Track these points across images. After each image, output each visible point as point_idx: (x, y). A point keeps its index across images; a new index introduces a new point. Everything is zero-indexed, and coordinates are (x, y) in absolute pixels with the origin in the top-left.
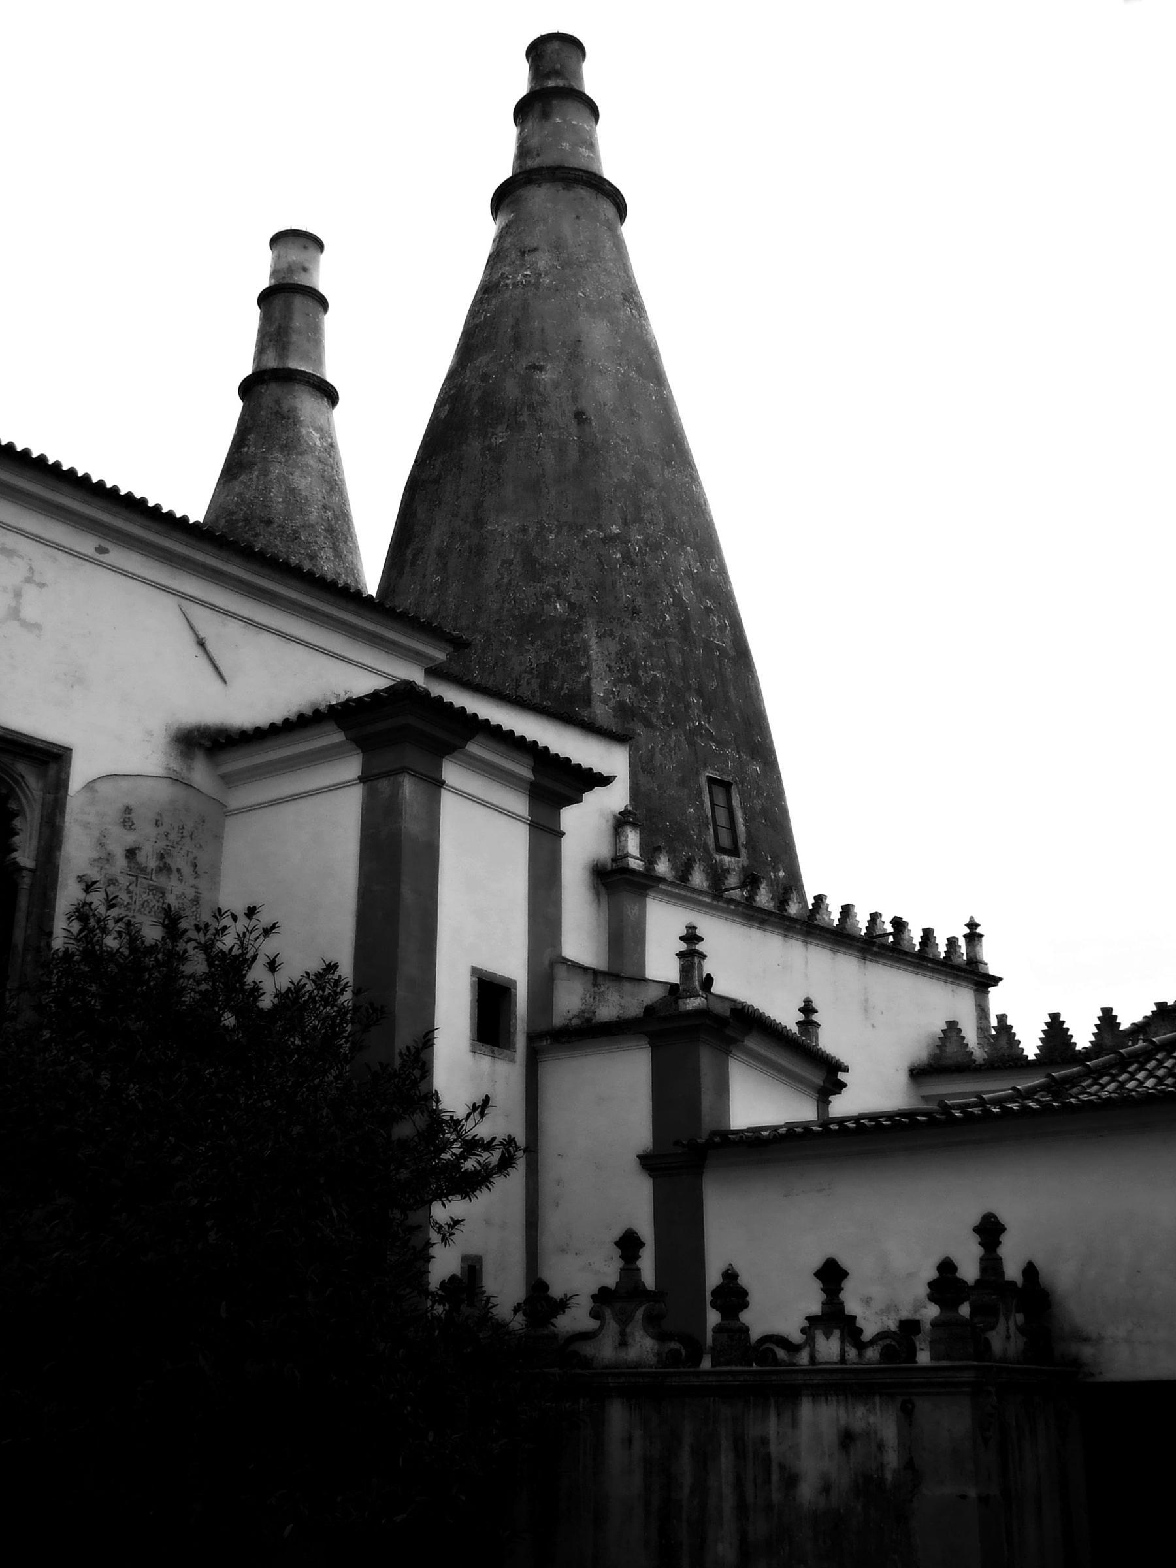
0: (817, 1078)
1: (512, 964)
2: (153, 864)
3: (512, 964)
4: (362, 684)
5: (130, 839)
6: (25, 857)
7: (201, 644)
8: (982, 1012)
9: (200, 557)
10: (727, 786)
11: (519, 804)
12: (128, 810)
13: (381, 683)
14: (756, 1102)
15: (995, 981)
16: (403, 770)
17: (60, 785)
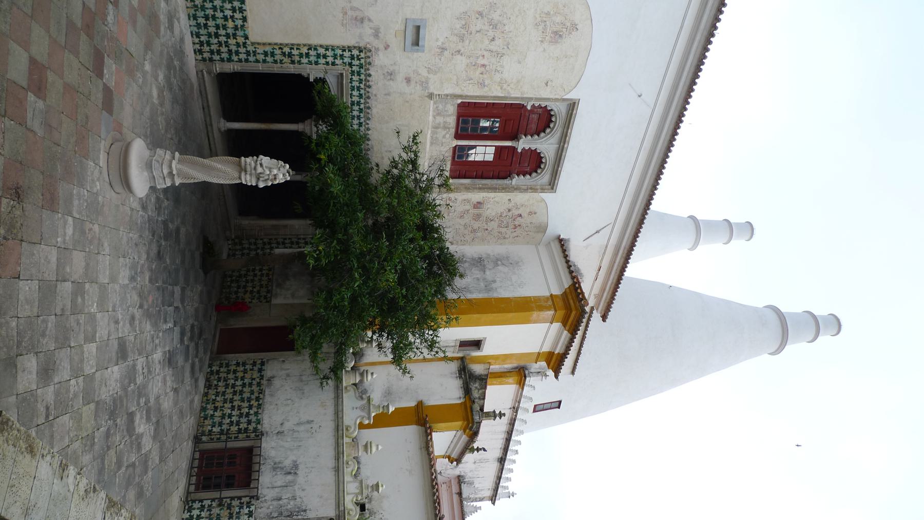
0: (454, 455)
1: (487, 350)
2: (517, 223)
4: (586, 287)
6: (517, 180)
7: (597, 232)
8: (481, 500)
9: (630, 228)
10: (559, 407)
11: (546, 348)
12: (535, 213)
13: (586, 295)
15: (494, 504)
16: (556, 311)
17: (543, 190)
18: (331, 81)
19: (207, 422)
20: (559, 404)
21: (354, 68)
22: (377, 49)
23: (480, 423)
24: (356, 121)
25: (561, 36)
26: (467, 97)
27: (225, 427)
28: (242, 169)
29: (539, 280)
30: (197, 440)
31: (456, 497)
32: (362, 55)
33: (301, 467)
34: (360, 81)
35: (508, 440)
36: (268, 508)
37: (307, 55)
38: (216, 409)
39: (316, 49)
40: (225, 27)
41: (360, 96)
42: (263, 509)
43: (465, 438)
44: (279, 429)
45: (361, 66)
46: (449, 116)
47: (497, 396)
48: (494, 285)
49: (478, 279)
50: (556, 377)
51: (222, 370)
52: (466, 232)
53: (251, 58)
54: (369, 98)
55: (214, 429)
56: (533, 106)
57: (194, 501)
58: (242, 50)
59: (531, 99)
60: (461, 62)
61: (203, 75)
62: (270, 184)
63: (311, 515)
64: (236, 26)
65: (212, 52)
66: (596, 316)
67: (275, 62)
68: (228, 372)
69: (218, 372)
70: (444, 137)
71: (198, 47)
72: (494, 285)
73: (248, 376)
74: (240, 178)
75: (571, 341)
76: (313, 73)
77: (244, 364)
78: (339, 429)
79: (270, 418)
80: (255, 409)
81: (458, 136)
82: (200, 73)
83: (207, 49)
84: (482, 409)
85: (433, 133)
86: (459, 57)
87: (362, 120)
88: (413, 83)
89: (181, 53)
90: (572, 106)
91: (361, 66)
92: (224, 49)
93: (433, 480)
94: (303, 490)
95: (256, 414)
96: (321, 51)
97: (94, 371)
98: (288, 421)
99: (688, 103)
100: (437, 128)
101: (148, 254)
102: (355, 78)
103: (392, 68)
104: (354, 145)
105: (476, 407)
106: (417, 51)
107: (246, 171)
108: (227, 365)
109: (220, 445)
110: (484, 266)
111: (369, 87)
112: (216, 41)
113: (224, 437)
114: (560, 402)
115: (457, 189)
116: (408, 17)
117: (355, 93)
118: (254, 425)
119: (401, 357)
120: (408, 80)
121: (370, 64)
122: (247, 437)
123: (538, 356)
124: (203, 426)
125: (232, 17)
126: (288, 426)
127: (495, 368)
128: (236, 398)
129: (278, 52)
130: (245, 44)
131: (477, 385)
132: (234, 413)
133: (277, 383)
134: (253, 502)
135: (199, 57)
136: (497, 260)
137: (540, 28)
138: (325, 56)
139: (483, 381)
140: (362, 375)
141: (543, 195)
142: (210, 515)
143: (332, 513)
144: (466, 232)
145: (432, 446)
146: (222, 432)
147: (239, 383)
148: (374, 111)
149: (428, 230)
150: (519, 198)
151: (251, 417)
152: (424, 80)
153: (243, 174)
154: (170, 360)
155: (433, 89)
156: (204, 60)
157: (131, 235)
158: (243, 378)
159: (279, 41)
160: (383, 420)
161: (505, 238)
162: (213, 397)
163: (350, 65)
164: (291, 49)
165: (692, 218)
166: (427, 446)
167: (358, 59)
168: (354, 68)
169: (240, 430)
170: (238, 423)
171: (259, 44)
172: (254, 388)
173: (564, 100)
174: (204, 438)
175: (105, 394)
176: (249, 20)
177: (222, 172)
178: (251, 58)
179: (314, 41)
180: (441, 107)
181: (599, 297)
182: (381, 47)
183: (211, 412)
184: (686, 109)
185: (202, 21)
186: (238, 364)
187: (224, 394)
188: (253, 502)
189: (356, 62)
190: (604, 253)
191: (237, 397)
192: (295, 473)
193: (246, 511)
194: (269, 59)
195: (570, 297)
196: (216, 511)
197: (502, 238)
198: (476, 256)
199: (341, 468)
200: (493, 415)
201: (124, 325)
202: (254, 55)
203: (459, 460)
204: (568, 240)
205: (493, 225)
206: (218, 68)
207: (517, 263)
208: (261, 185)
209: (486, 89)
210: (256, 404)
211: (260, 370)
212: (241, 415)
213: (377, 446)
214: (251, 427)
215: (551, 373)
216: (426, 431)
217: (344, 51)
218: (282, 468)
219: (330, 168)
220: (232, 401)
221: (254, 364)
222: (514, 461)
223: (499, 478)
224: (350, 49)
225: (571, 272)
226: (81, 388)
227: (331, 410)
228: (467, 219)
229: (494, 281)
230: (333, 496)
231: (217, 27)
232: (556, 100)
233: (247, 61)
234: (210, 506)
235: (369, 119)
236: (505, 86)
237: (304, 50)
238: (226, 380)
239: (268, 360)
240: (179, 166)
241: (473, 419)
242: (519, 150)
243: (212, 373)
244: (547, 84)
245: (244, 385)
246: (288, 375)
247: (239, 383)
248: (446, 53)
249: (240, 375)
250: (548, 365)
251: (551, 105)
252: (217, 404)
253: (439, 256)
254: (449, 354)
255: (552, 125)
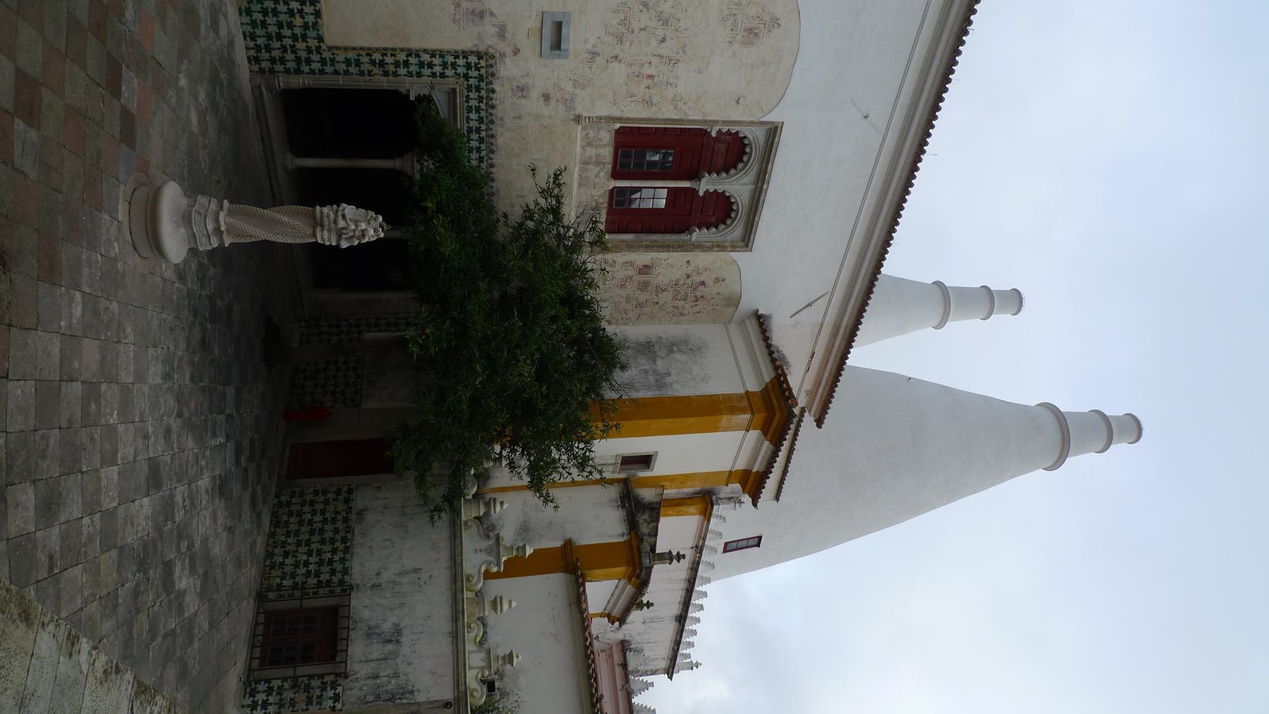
1: (659, 469)
2: (698, 294)
3: (660, 469)
4: (794, 380)
5: (709, 282)
6: (697, 235)
7: (809, 305)
8: (654, 673)
10: (758, 545)
11: (741, 465)
13: (795, 392)
14: (599, 593)
15: (671, 678)
16: (753, 414)
17: (734, 248)
18: (440, 98)
19: (274, 573)
20: (758, 541)
21: (472, 81)
22: (503, 55)
23: (650, 568)
24: (474, 155)
25: (756, 35)
26: (627, 120)
27: (299, 579)
28: (317, 223)
29: (728, 371)
30: (261, 597)
31: (618, 670)
32: (483, 63)
33: (405, 632)
34: (480, 99)
35: (689, 591)
36: (361, 689)
37: (406, 64)
38: (286, 554)
39: (417, 55)
40: (290, 26)
41: (480, 120)
42: (354, 691)
43: (630, 589)
44: (375, 581)
45: (480, 78)
46: (604, 146)
47: (674, 532)
48: (668, 380)
49: (646, 372)
50: (755, 504)
51: (294, 500)
52: (629, 307)
53: (328, 69)
54: (492, 122)
55: (285, 583)
56: (719, 132)
57: (258, 682)
58: (315, 57)
59: (716, 122)
60: (619, 72)
61: (261, 92)
62: (356, 243)
63: (420, 698)
64: (306, 24)
65: (273, 60)
66: (809, 420)
67: (362, 73)
68: (303, 504)
69: (289, 504)
70: (597, 176)
71: (253, 53)
72: (668, 380)
73: (330, 508)
74: (314, 235)
75: (775, 455)
76: (415, 88)
77: (325, 492)
78: (457, 580)
79: (363, 565)
80: (340, 555)
81: (616, 175)
82: (256, 89)
83: (267, 56)
84: (653, 548)
85: (582, 170)
86: (616, 64)
87: (483, 153)
88: (553, 102)
89: (228, 62)
90: (774, 131)
91: (480, 78)
92: (290, 56)
93: (587, 648)
94: (409, 664)
95: (343, 560)
96: (426, 58)
97: (114, 504)
98: (387, 569)
99: (933, 127)
100: (587, 163)
101: (188, 341)
102: (473, 95)
103: (523, 81)
104: (473, 188)
105: (646, 547)
106: (559, 57)
107: (322, 226)
108: (302, 494)
109: (294, 604)
110: (654, 353)
111: (493, 107)
112: (278, 45)
113: (298, 593)
114: (760, 538)
115: (617, 248)
116: (545, 9)
117: (473, 116)
118: (339, 576)
119: (541, 480)
120: (546, 97)
121: (493, 75)
122: (331, 592)
123: (730, 477)
124: (268, 579)
125: (300, 11)
126: (387, 576)
127: (670, 492)
128: (314, 539)
129: (365, 59)
130: (318, 48)
131: (646, 516)
132: (312, 560)
133: (370, 517)
134: (340, 681)
135: (256, 68)
136: (672, 344)
137: (729, 23)
138: (431, 65)
139: (654, 511)
140: (487, 505)
141: (734, 255)
142: (281, 700)
143: (448, 695)
144: (629, 307)
145: (586, 601)
146: (295, 587)
147: (318, 518)
148: (500, 141)
149: (577, 305)
150: (702, 259)
151: (335, 565)
152: (567, 97)
153: (318, 230)
154: (221, 488)
155: (582, 108)
156: (262, 71)
157: (164, 316)
158: (323, 512)
159: (367, 45)
160: (518, 567)
161: (682, 315)
162: (283, 538)
163: (466, 77)
164: (384, 55)
165: (938, 284)
166: (578, 600)
167: (477, 69)
168: (472, 81)
169: (320, 582)
170: (317, 574)
171: (338, 48)
172: (339, 525)
173: (762, 123)
174: (271, 595)
175: (131, 537)
176: (325, 16)
177: (288, 227)
178: (328, 69)
179: (416, 44)
180: (592, 134)
181: (812, 395)
182: (509, 51)
183: (281, 559)
184: (929, 135)
185: (258, 17)
186: (316, 493)
187: (297, 533)
188: (340, 681)
189: (473, 73)
190: (819, 334)
191: (315, 538)
192: (398, 641)
193: (331, 694)
194: (353, 69)
195: (772, 394)
196: (288, 695)
197: (678, 314)
198: (642, 339)
199: (460, 632)
200: (669, 557)
201: (157, 440)
202: (333, 64)
203: (622, 620)
204: (767, 317)
205: (666, 297)
206: (282, 82)
207: (699, 349)
208: (344, 245)
209: (654, 109)
210: (341, 547)
211: (347, 501)
212: (321, 563)
213: (510, 602)
214: (335, 579)
215: (747, 499)
216: (577, 581)
217: (457, 57)
218: (379, 635)
219: (438, 221)
220: (308, 543)
221: (339, 492)
222: (698, 620)
223: (677, 643)
224: (465, 54)
225: (773, 361)
226: (98, 528)
227: (444, 555)
228: (631, 289)
229: (669, 374)
230: (450, 671)
231: (280, 25)
232: (752, 123)
233: (322, 72)
234: (279, 688)
235: (492, 152)
236: (680, 105)
237: (402, 57)
238: (299, 514)
239: (357, 487)
240: (230, 220)
241: (641, 563)
242: (701, 193)
243: (280, 505)
244: (738, 102)
245: (325, 521)
246: (386, 507)
247: (318, 518)
248: (598, 59)
249: (319, 507)
250: (744, 488)
251: (744, 131)
252: (288, 548)
253: (591, 340)
254: (608, 475)
255: (745, 159)
